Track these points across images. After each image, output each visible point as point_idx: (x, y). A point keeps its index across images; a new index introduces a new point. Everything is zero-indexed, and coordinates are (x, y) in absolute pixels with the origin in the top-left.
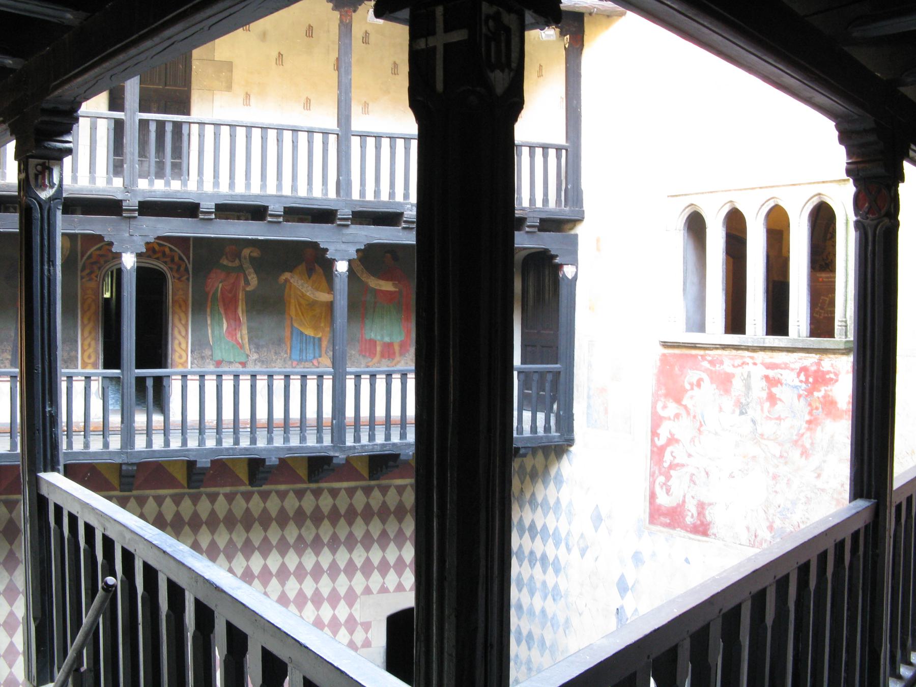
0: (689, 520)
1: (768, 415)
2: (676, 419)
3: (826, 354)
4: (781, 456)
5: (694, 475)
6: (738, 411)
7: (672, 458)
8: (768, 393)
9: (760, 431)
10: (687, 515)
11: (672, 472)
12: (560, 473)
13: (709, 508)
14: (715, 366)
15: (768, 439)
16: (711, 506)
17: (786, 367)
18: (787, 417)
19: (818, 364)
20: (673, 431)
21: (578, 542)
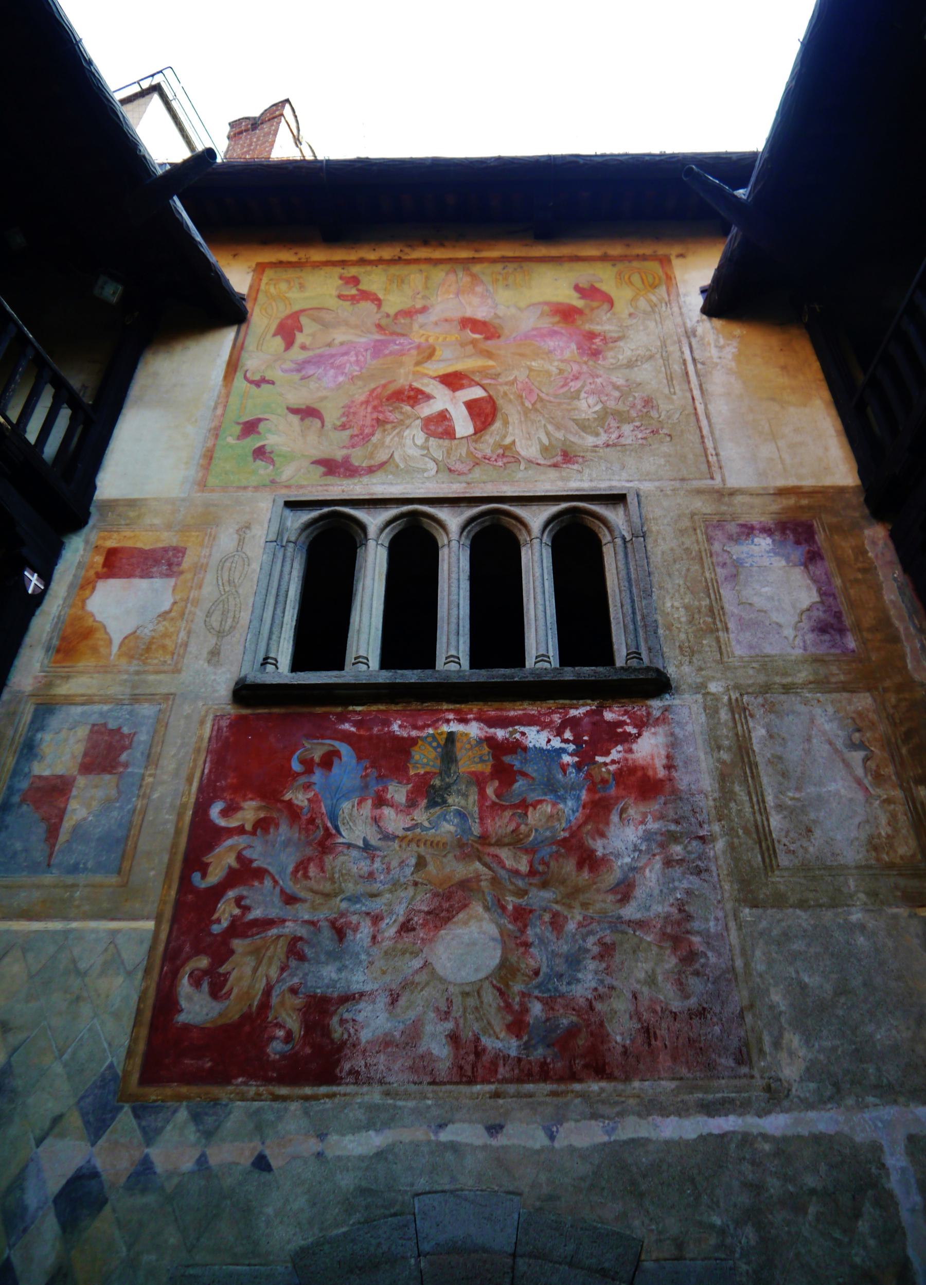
0: (276, 1048)
1: (497, 801)
2: (259, 831)
4: (532, 873)
5: (301, 939)
6: (424, 802)
7: (237, 911)
8: (493, 766)
10: (273, 1038)
11: (238, 944)
13: (342, 1009)
14: (371, 729)
15: (499, 843)
17: (530, 721)
18: (540, 802)
20: (247, 853)
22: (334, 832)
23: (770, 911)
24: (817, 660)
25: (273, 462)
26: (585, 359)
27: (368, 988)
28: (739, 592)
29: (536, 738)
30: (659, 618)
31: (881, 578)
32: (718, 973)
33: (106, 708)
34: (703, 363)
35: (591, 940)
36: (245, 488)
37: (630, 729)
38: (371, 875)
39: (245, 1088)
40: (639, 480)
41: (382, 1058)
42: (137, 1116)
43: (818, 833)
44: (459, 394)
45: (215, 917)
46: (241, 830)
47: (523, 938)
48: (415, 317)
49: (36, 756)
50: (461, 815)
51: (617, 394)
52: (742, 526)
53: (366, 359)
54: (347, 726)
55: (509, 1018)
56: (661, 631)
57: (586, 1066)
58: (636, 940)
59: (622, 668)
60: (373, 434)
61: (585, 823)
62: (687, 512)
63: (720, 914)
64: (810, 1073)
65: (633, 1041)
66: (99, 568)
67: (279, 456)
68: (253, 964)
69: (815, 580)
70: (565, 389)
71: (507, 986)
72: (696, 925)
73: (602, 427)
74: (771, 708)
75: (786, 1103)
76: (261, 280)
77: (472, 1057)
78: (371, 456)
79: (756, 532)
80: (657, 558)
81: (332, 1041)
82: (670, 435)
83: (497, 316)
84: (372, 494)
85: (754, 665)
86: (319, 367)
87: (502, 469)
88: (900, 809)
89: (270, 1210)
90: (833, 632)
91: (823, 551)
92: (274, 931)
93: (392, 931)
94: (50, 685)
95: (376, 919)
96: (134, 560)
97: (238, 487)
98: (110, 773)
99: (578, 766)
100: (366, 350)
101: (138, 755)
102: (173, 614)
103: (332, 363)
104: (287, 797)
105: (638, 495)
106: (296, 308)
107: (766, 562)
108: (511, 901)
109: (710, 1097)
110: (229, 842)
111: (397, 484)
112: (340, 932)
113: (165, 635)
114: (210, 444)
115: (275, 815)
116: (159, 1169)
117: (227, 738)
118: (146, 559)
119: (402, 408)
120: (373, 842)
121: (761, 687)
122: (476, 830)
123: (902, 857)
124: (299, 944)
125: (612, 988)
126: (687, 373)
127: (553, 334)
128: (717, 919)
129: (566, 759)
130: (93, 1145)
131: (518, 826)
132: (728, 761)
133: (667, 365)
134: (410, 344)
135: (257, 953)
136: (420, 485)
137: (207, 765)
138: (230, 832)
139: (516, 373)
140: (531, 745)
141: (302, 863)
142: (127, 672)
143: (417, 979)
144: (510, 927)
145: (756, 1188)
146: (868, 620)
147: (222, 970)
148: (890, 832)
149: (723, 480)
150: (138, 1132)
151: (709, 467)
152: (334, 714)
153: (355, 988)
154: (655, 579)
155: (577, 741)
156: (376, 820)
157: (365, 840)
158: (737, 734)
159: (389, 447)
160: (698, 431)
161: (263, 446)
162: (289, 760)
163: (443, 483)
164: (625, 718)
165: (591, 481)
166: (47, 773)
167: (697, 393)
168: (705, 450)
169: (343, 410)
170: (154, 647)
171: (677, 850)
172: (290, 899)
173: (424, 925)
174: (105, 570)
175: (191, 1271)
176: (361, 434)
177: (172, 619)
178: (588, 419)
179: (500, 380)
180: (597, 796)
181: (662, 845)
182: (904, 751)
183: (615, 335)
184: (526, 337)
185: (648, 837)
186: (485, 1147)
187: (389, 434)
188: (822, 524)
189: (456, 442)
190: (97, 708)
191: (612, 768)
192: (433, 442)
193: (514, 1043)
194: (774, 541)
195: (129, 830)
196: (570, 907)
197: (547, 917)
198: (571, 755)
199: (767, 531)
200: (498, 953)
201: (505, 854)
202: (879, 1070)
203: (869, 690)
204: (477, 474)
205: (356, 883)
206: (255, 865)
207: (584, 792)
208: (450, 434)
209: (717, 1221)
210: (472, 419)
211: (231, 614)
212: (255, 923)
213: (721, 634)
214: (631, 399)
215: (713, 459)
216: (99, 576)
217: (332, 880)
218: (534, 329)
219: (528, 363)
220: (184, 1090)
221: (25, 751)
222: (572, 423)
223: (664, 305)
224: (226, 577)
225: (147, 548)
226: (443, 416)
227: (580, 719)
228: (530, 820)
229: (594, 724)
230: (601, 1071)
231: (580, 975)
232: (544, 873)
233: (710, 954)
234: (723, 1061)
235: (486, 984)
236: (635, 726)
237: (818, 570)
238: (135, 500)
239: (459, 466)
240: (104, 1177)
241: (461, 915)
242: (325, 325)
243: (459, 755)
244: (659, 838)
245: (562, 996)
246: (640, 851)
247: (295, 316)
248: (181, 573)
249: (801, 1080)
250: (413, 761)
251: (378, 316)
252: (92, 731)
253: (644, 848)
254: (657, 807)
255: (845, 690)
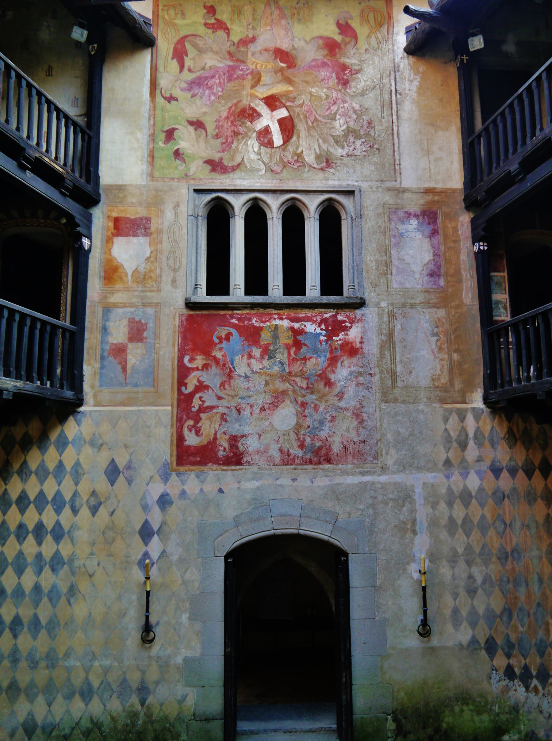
2: (204, 369)
3: (342, 309)
4: (308, 388)
5: (225, 414)
6: (267, 357)
7: (201, 403)
8: (293, 341)
9: (287, 370)
10: (220, 450)
11: (202, 415)
12: (63, 435)
13: (242, 440)
14: (244, 322)
15: (296, 376)
16: (244, 438)
17: (308, 319)
18: (311, 358)
19: (335, 316)
20: (201, 379)
21: (87, 501)
22: (233, 370)
23: (392, 405)
24: (427, 291)
25: (184, 161)
26: (340, 87)
27: (250, 432)
28: (399, 252)
29: (310, 328)
30: (364, 266)
31: (462, 247)
32: (370, 428)
33: (133, 310)
34: (400, 94)
35: (328, 415)
36: (173, 179)
37: (348, 324)
38: (248, 388)
39: (212, 467)
40: (361, 181)
41: (257, 457)
42: (178, 476)
43: (413, 373)
44: (275, 113)
45: (193, 405)
46: (197, 369)
47: (304, 414)
48: (249, 47)
49: (108, 333)
50: (282, 363)
51: (354, 116)
52: (406, 212)
53: (224, 81)
54: (234, 321)
55: (299, 443)
56: (364, 274)
57: (324, 460)
58: (344, 415)
59: (347, 297)
60: (232, 143)
61: (328, 367)
62: (382, 202)
63: (374, 406)
64: (396, 463)
65: (340, 452)
66: (112, 230)
67: (187, 157)
68: (209, 423)
69: (433, 247)
70: (329, 112)
71: (298, 431)
72: (365, 410)
73: (346, 142)
74: (404, 315)
75: (387, 472)
76: (158, 6)
77: (287, 457)
78: (232, 159)
79: (412, 216)
80: (365, 232)
81: (240, 451)
82: (378, 149)
83: (294, 48)
84: (235, 186)
85: (401, 293)
86: (200, 88)
87: (297, 171)
88: (445, 363)
89: (225, 505)
90: (435, 276)
91: (439, 229)
92: (215, 411)
93: (258, 411)
94: (105, 297)
95: (252, 406)
96: (128, 225)
97: (170, 178)
98: (141, 342)
99: (326, 341)
100: (224, 74)
101: (151, 333)
102: (152, 259)
103: (207, 84)
104: (213, 354)
105: (360, 191)
106: (182, 34)
107: (412, 235)
108: (300, 399)
109: (363, 470)
110: (193, 374)
111: (246, 179)
112: (239, 411)
113: (150, 271)
114: (151, 147)
115: (210, 362)
116: (188, 492)
117: (186, 326)
118: (133, 224)
119: (246, 123)
120: (249, 374)
121: (402, 304)
122: (287, 370)
123: (442, 384)
124: (225, 416)
125: (334, 433)
126: (391, 101)
127: (324, 64)
128: (373, 407)
129: (322, 338)
130: (165, 485)
131: (303, 368)
132: (384, 340)
133: (382, 95)
134: (248, 70)
135: (210, 419)
136: (258, 180)
137: (180, 339)
138: (194, 369)
139: (303, 97)
140: (308, 331)
141: (222, 383)
142: (138, 291)
143: (267, 429)
144: (300, 409)
145: (374, 498)
146: (451, 271)
147: (198, 425)
148: (440, 373)
149: (401, 182)
150: (179, 482)
151: (395, 173)
152: (228, 314)
153: (246, 432)
154: (364, 243)
155: (326, 330)
156: (249, 365)
157: (245, 373)
158: (389, 328)
159: (241, 152)
160: (392, 148)
161: (178, 150)
162: (212, 337)
163: (269, 179)
164: (346, 319)
165: (339, 180)
166: (115, 342)
167: (395, 117)
168: (395, 160)
169: (216, 124)
170: (147, 277)
171: (361, 379)
172: (219, 398)
173: (269, 408)
174: (115, 231)
175: (203, 522)
176: (227, 142)
177: (152, 262)
178: (340, 136)
179: (295, 103)
180: (333, 355)
181: (356, 377)
182: (452, 337)
183: (357, 68)
184: (310, 68)
185: (351, 373)
186: (291, 486)
187: (241, 143)
188: (442, 212)
189: (274, 150)
190: (129, 309)
191: (340, 342)
192: (263, 149)
193: (301, 451)
194: (419, 222)
195: (154, 368)
196: (321, 402)
197: (313, 406)
198: (324, 336)
199: (416, 216)
200: (296, 419)
201: (298, 380)
202: (419, 462)
203: (445, 307)
204: (285, 174)
205: (243, 392)
206: (204, 384)
207: (328, 353)
208: (270, 144)
209: (361, 507)
210: (282, 133)
211: (178, 259)
212: (208, 407)
213: (389, 276)
214: (361, 121)
215: (397, 167)
216: (114, 235)
217: (234, 390)
218: (314, 60)
219: (310, 89)
220: (192, 467)
221: (104, 331)
222: (331, 138)
223: (385, 42)
224: (172, 238)
225: (133, 217)
226: (266, 131)
227: (328, 319)
228: (307, 366)
229: (333, 321)
230: (329, 461)
231: (323, 428)
232: (312, 388)
233: (369, 421)
234: (369, 458)
235: (291, 431)
236: (350, 323)
237: (435, 240)
238: (121, 186)
239: (276, 168)
240: (171, 494)
241: (282, 405)
242: (201, 51)
243: (280, 335)
244: (355, 374)
245: (317, 435)
246: (348, 379)
247: (182, 41)
248: (151, 234)
249: (393, 465)
250: (262, 338)
251: (228, 44)
252: (129, 322)
253: (349, 378)
254: (355, 360)
255: (435, 307)
